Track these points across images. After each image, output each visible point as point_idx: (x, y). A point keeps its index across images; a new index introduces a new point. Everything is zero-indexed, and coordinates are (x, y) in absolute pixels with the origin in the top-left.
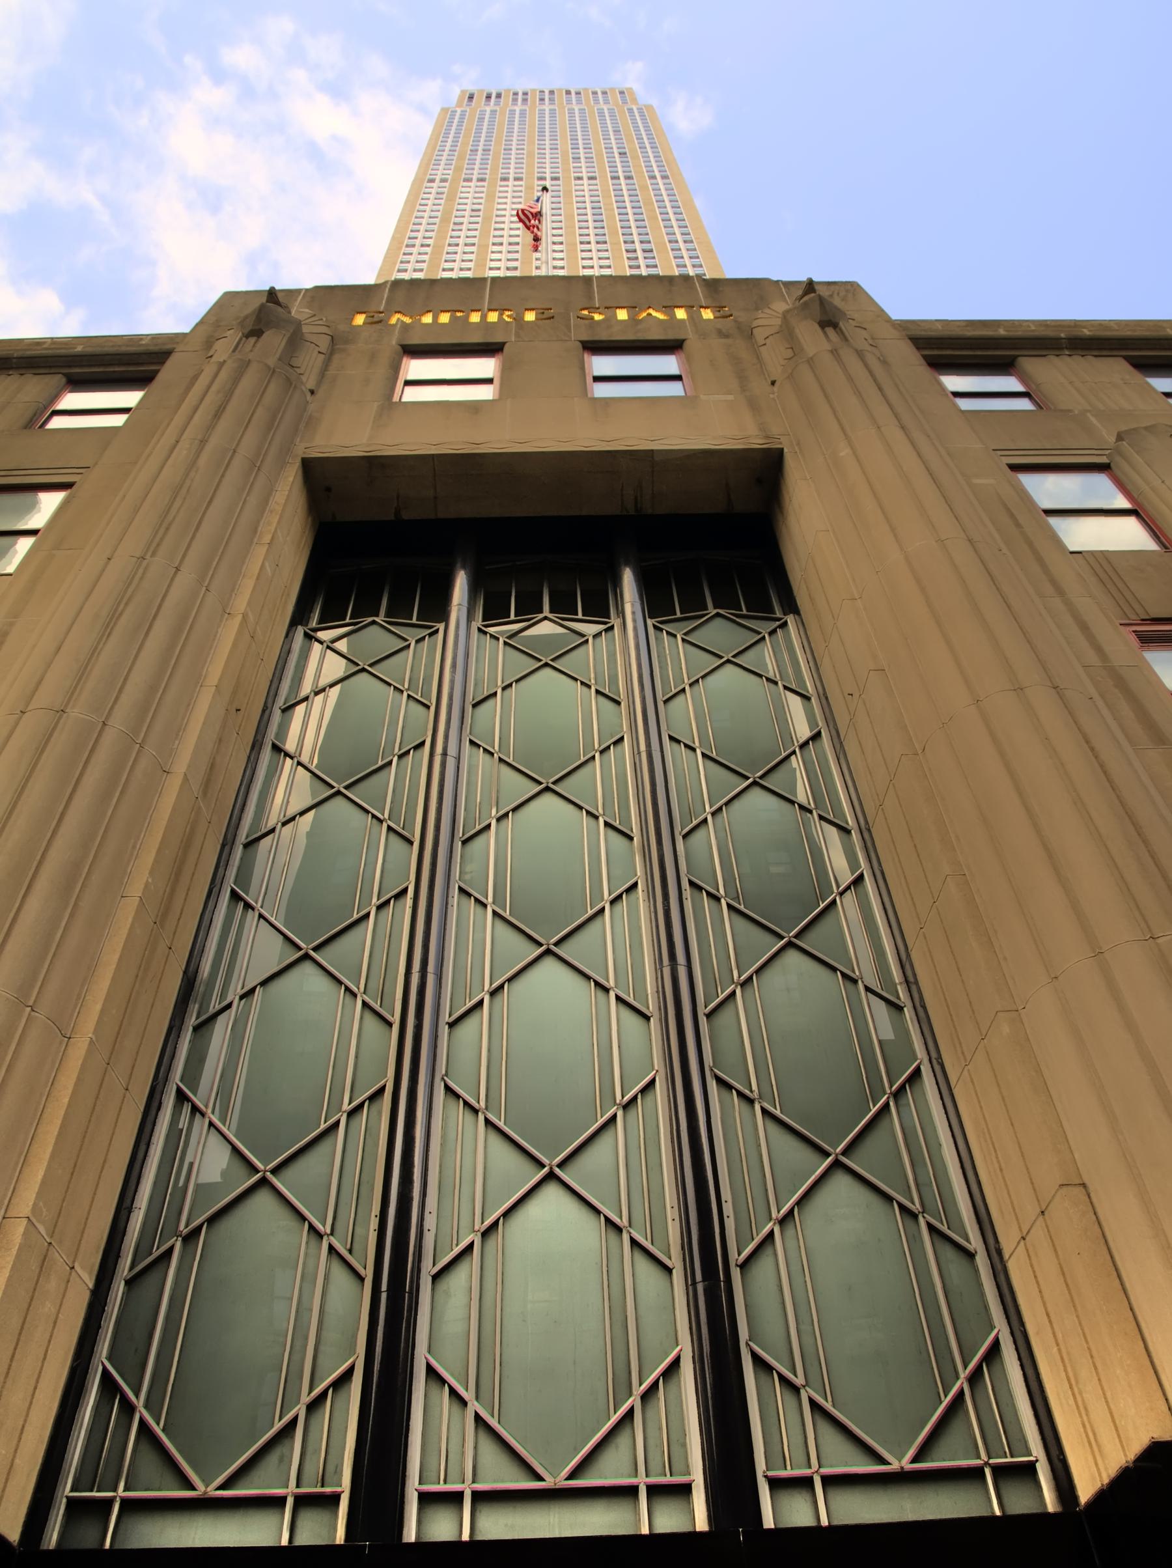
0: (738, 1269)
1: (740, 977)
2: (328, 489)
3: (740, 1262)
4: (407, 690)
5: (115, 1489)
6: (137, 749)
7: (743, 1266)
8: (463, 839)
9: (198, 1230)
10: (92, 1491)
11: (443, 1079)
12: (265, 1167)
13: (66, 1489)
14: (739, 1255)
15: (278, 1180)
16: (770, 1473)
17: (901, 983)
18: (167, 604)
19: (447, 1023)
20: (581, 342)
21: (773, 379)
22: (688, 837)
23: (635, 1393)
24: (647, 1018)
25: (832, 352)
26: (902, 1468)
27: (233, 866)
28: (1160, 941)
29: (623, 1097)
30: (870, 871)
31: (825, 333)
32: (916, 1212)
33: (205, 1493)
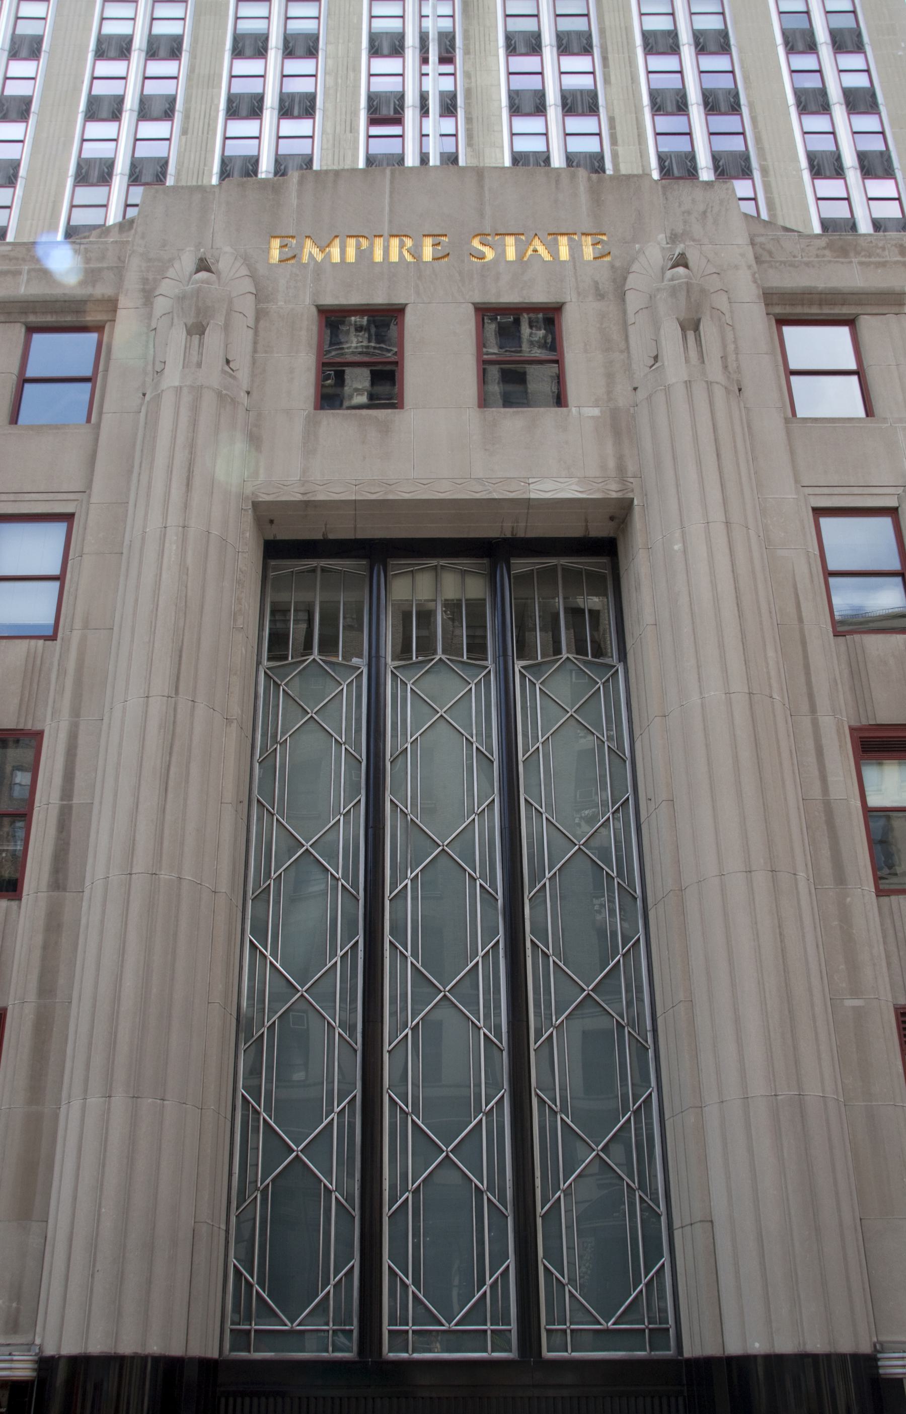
4: (345, 743)
11: (388, 1092)
17: (650, 1031)
19: (388, 1051)
20: (473, 304)
21: (636, 386)
24: (502, 1051)
25: (686, 382)
28: (779, 1098)
29: (486, 1107)
30: (644, 937)
31: (685, 337)
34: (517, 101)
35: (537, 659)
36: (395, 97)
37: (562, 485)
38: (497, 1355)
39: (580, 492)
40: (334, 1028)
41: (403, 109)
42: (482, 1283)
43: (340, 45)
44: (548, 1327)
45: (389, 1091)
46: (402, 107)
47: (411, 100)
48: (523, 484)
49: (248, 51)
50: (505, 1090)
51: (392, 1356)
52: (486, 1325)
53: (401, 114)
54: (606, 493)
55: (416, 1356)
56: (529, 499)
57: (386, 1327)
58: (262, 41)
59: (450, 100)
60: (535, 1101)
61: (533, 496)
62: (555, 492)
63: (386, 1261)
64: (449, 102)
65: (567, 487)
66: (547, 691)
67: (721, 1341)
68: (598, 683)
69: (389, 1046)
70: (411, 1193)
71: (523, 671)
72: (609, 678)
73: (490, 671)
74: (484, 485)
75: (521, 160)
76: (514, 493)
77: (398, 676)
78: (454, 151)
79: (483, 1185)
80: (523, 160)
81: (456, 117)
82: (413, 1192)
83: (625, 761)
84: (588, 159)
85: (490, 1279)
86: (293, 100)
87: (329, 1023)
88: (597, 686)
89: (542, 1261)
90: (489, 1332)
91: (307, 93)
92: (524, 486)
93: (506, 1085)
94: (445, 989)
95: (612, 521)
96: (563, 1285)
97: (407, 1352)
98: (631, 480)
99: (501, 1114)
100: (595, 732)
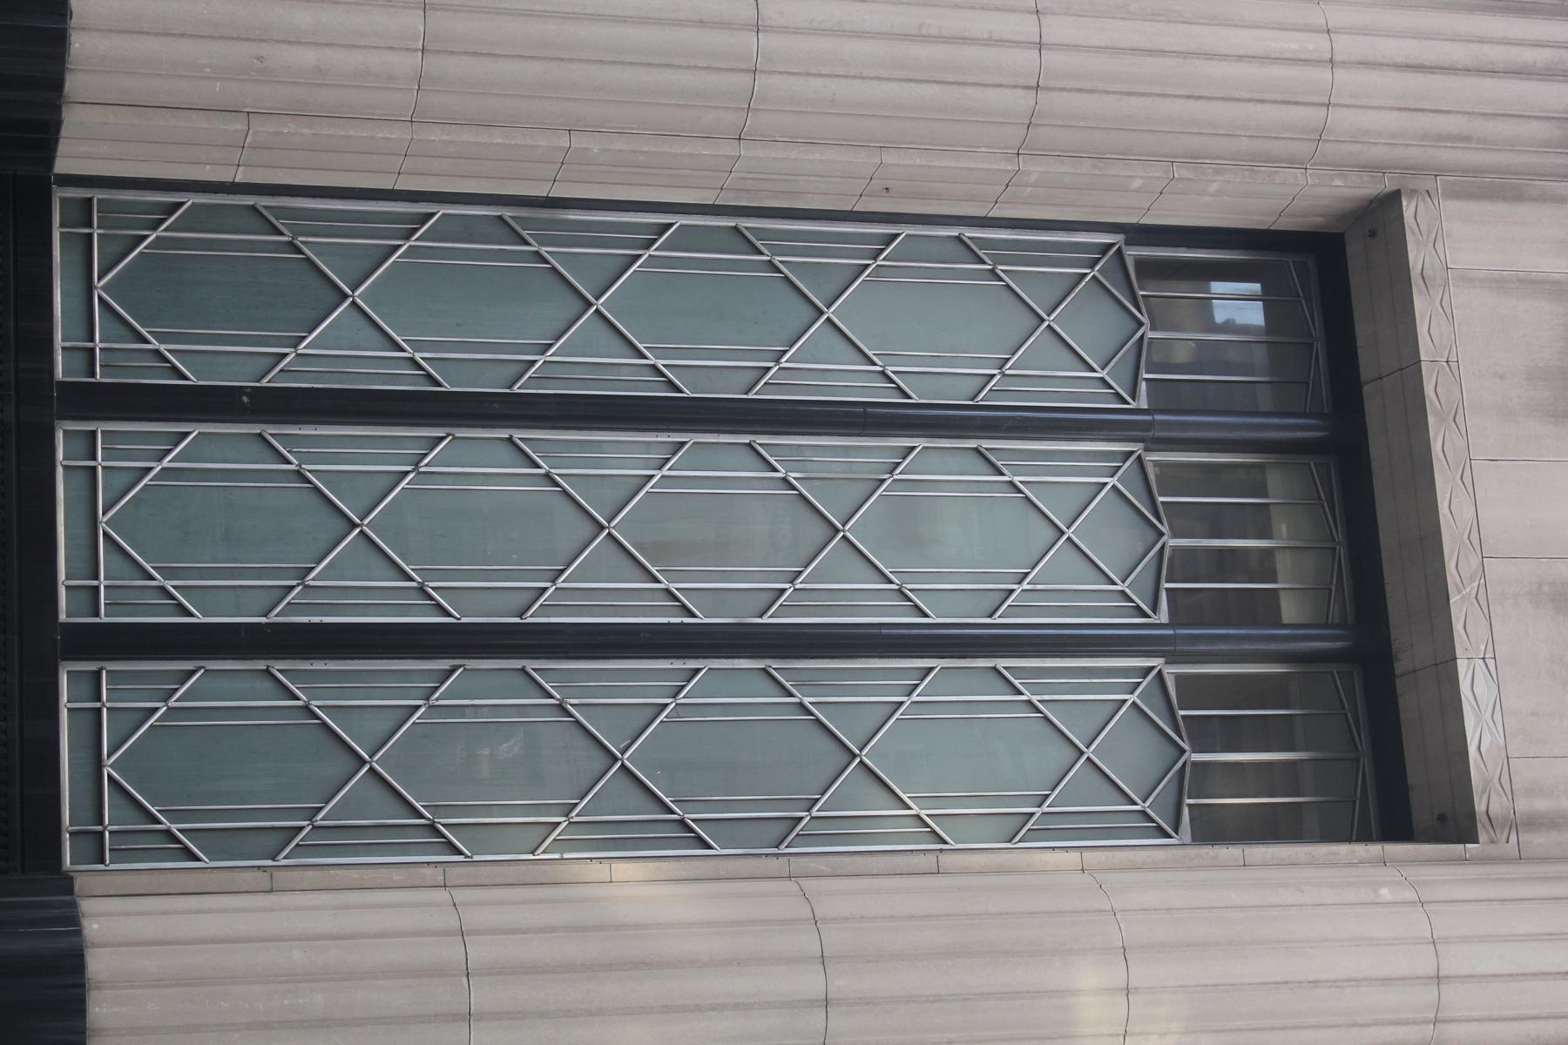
0: (265, 668)
1: (571, 705)
2: (1373, 234)
3: (271, 670)
5: (98, 227)
6: (742, 106)
7: (267, 671)
8: (753, 444)
9: (300, 252)
10: (98, 212)
11: (448, 435)
12: (358, 297)
13: (98, 195)
14: (279, 671)
15: (348, 306)
16: (104, 672)
18: (969, 90)
19: (511, 436)
22: (764, 674)
23: (166, 582)
24: (520, 616)
26: (104, 766)
27: (705, 220)
29: (433, 588)
32: (314, 819)
33: (96, 288)
35: (1180, 709)
37: (1488, 716)
38: (62, 593)
39: (1479, 747)
40: (542, 354)
42: (169, 573)
44: (104, 672)
45: (451, 437)
48: (1483, 647)
50: (459, 619)
51: (60, 436)
52: (105, 579)
54: (1483, 792)
55: (60, 471)
56: (1456, 658)
57: (100, 427)
60: (444, 664)
61: (1462, 666)
62: (1475, 706)
63: (195, 429)
65: (1484, 723)
66: (1121, 713)
67: (95, 893)
68: (1144, 802)
69: (520, 439)
70: (297, 468)
71: (1155, 672)
72: (1154, 821)
73: (1148, 617)
74: (1472, 580)
76: (1462, 632)
77: (1124, 462)
79: (312, 580)
82: (298, 471)
83: (1010, 841)
85: (174, 587)
87: (551, 345)
88: (1139, 801)
89: (202, 668)
90: (95, 583)
92: (1479, 648)
93: (464, 620)
94: (614, 528)
95: (1438, 819)
96: (166, 700)
97: (64, 459)
98: (1513, 838)
99: (419, 610)
100: (1057, 792)
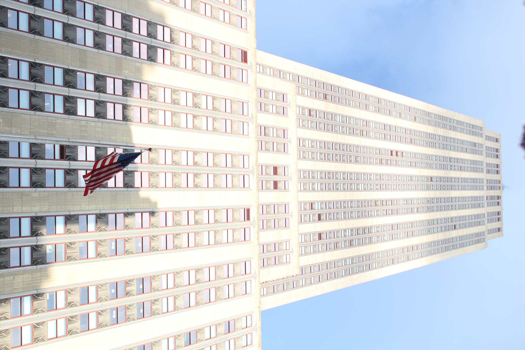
34: (72, 219)
36: (74, 156)
41: (68, 160)
43: (101, 129)
46: (69, 160)
47: (73, 165)
49: (98, 83)
53: (66, 159)
58: (103, 90)
59: (73, 185)
64: (72, 184)
75: (42, 221)
78: (47, 186)
80: (42, 222)
81: (65, 187)
84: (42, 256)
86: (73, 103)
91: (77, 111)
